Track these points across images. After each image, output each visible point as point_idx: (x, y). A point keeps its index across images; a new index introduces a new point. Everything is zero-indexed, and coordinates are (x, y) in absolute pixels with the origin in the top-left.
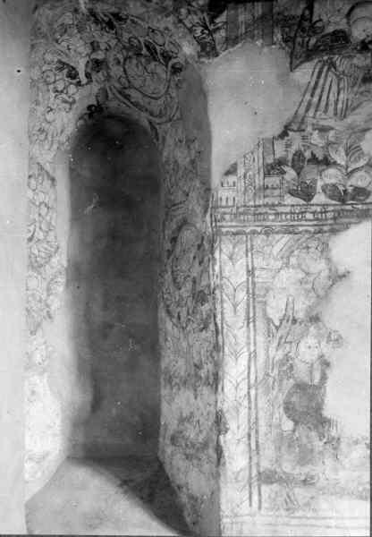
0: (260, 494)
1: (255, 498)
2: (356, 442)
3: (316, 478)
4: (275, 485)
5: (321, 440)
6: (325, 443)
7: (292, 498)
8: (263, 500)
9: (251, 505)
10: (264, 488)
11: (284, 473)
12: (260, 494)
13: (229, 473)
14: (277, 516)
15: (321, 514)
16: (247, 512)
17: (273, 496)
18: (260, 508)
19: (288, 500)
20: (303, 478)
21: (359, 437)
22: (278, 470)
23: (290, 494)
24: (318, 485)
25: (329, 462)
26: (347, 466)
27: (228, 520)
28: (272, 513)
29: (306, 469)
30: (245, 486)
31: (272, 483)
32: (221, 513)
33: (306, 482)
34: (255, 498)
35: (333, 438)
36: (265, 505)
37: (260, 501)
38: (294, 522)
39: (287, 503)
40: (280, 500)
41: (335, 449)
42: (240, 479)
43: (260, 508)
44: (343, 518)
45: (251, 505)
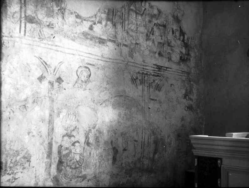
0: (25, 27)
1: (23, 29)
2: (72, 13)
3: (54, 25)
4: (34, 24)
5: (57, 7)
6: (59, 10)
7: (42, 33)
8: (27, 31)
9: (20, 32)
10: (28, 25)
11: (39, 20)
12: (25, 27)
13: (9, 13)
14: (34, 41)
15: (56, 44)
16: (18, 36)
17: (32, 30)
18: (25, 35)
19: (40, 33)
20: (48, 24)
21: (73, 11)
22: (36, 17)
23: (41, 30)
24: (55, 29)
25: (60, 19)
26: (67, 23)
27: (6, 38)
28: (30, 39)
29: (50, 20)
30: (18, 21)
31: (32, 23)
32: (3, 34)
33: (50, 26)
34: (23, 29)
35: (63, 8)
36: (27, 34)
37: (25, 31)
38: (43, 45)
39: (39, 36)
40: (36, 34)
41: (63, 14)
42: (15, 16)
43: (25, 35)
44: (64, 47)
45: (20, 32)
